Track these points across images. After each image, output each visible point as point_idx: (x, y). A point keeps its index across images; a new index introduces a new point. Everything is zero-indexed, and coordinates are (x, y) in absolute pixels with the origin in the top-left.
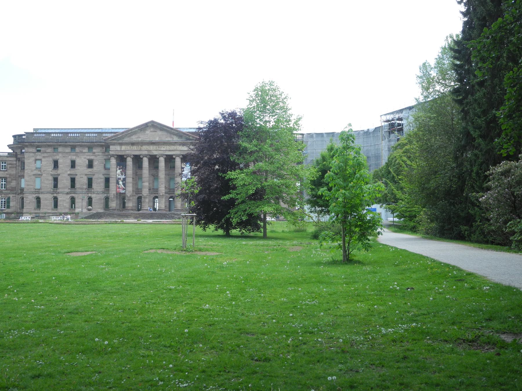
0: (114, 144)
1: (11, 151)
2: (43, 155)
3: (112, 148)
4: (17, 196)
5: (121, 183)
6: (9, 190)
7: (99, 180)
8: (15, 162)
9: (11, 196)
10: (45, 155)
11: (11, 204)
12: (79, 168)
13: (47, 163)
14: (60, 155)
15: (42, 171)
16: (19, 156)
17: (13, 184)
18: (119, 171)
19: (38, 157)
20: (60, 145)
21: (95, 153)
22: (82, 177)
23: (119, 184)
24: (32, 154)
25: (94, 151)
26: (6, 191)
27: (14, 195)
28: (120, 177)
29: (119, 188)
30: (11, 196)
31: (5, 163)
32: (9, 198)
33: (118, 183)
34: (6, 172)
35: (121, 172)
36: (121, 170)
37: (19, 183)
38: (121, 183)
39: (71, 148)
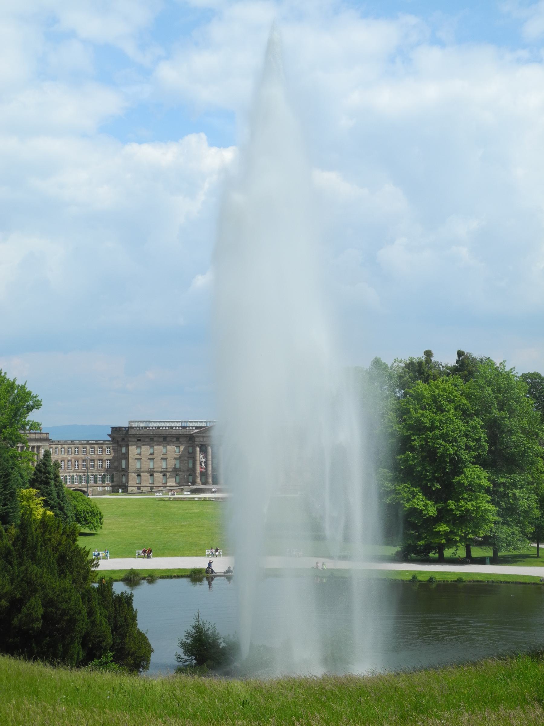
0: (198, 437)
1: (109, 439)
2: (142, 444)
3: (197, 439)
4: (119, 473)
5: (203, 464)
6: (113, 468)
7: (185, 462)
8: (117, 448)
9: (114, 473)
10: (144, 443)
11: (115, 479)
12: (169, 453)
13: (146, 450)
14: (155, 443)
15: (142, 455)
16: (120, 443)
17: (116, 464)
18: (201, 456)
19: (139, 445)
20: (156, 436)
21: (181, 442)
22: (172, 460)
23: (202, 465)
24: (134, 443)
25: (180, 440)
26: (110, 470)
27: (117, 472)
28: (202, 460)
29: (202, 468)
30: (114, 473)
31: (109, 448)
32: (113, 475)
33: (201, 464)
34: (111, 455)
35: (203, 456)
36: (203, 455)
37: (121, 464)
38: (203, 464)
39: (163, 438)
